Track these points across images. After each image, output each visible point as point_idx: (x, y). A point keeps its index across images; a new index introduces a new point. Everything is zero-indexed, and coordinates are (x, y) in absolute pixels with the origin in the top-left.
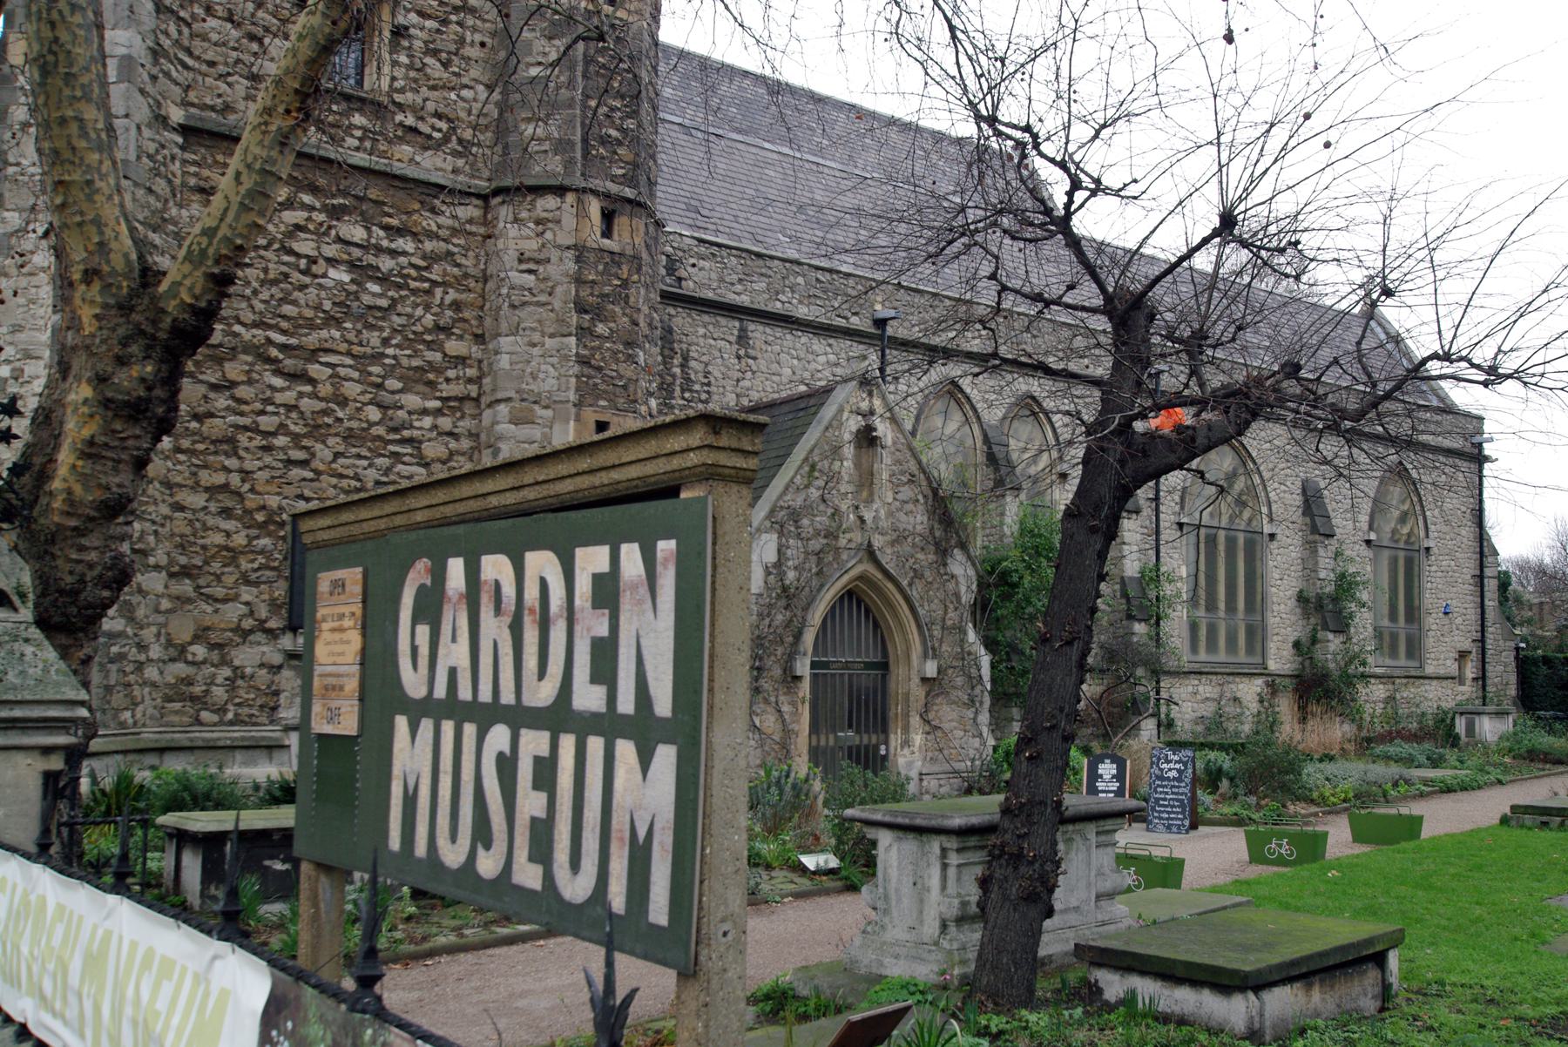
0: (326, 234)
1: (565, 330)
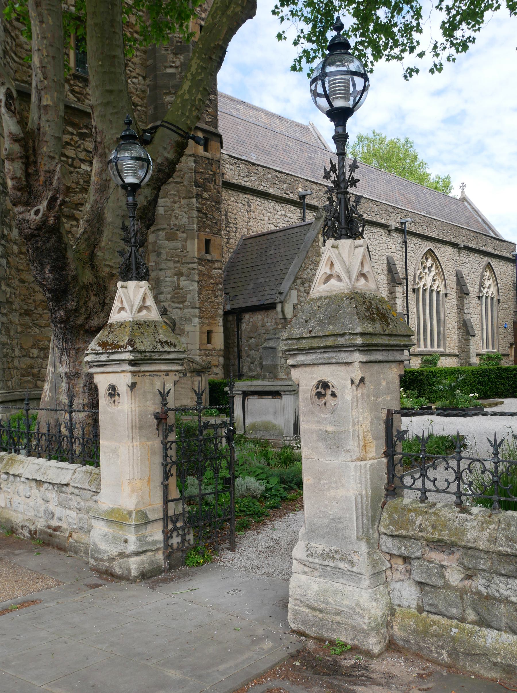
0: (79, 146)
1: (191, 196)
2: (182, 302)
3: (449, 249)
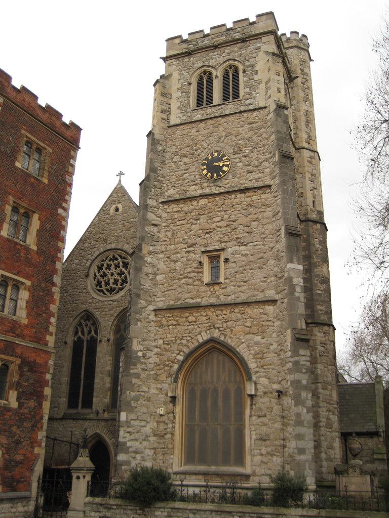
2: (331, 428)
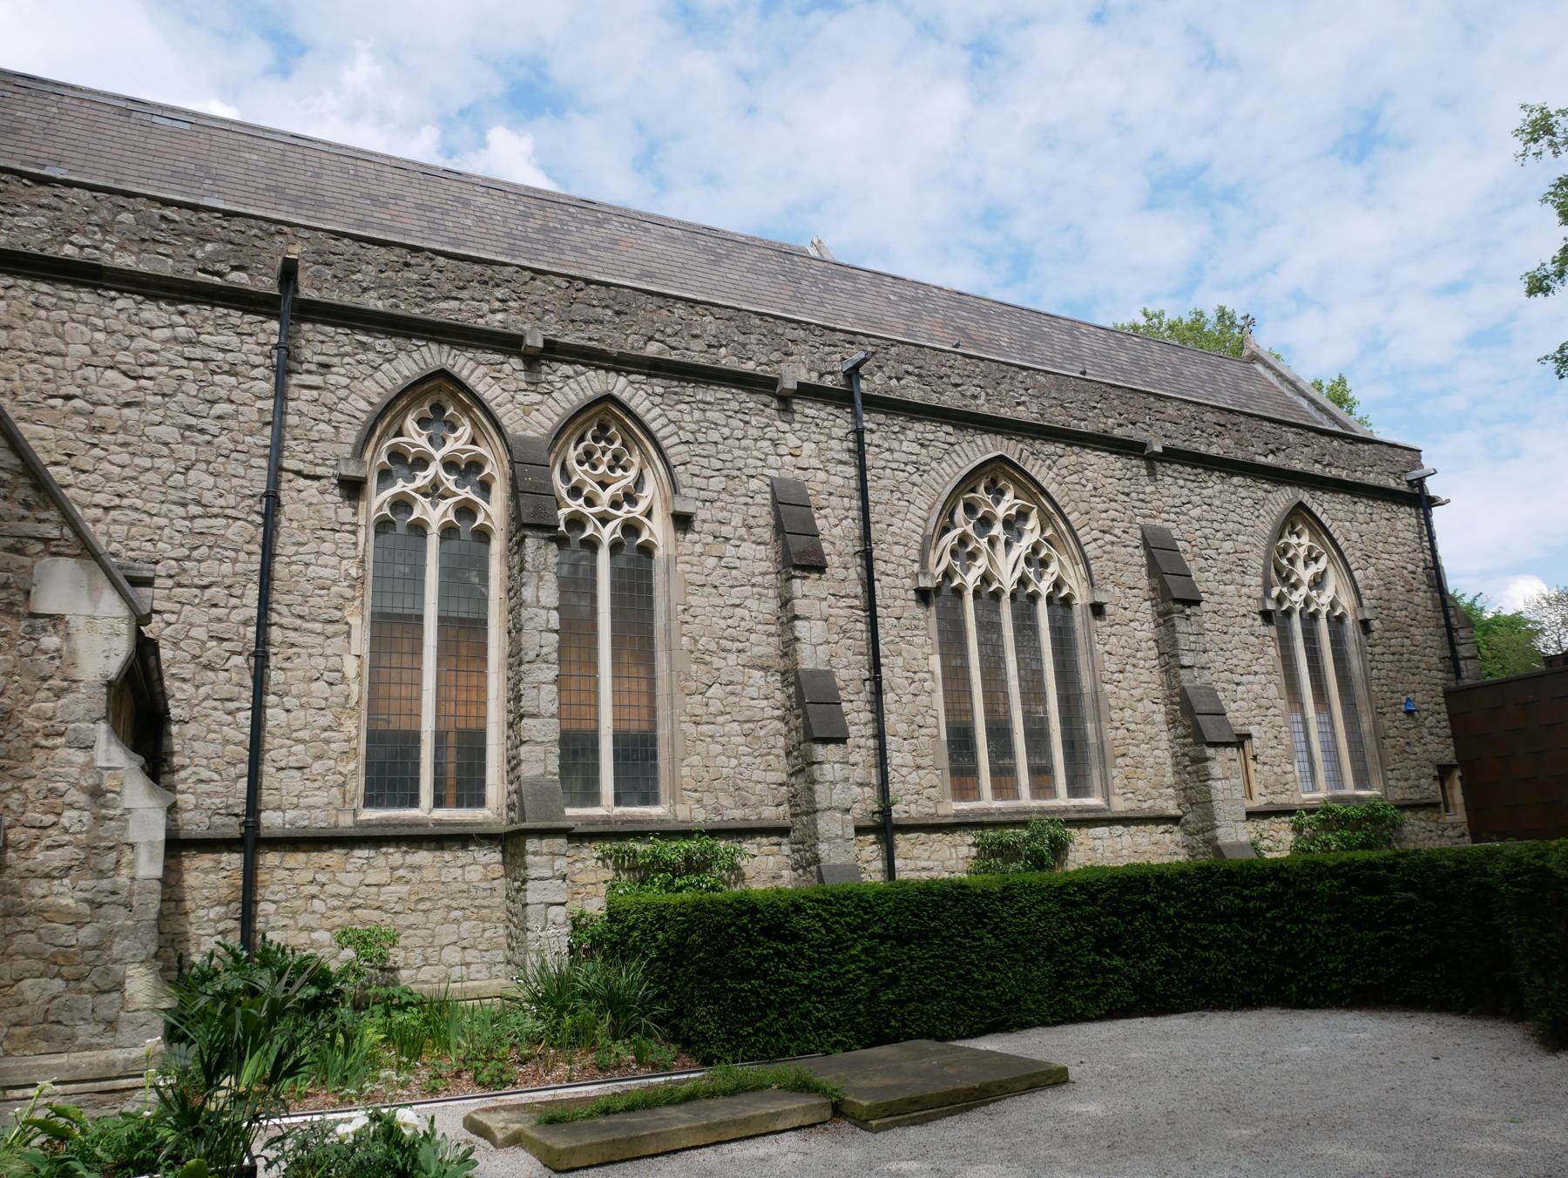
3: (1098, 463)
